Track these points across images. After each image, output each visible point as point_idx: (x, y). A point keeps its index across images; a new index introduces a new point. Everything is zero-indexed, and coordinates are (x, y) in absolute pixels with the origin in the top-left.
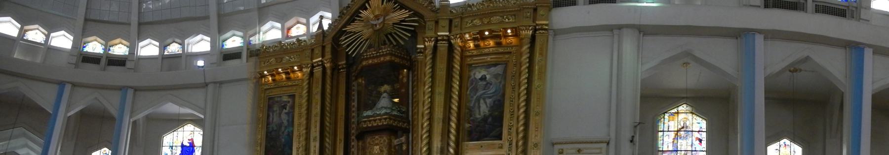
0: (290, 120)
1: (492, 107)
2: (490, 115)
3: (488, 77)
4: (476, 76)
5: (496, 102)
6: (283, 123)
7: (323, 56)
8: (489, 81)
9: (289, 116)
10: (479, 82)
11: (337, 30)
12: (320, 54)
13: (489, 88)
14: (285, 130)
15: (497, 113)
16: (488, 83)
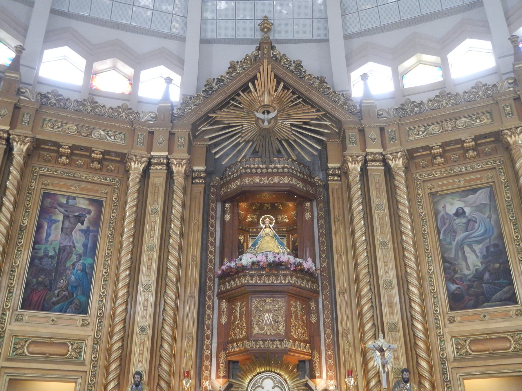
0: (89, 245)
1: (484, 257)
2: (486, 269)
3: (467, 210)
4: (447, 212)
5: (492, 249)
6: (74, 247)
7: (170, 150)
8: (469, 217)
9: (87, 238)
10: (455, 220)
11: (201, 114)
12: (166, 143)
13: (473, 229)
14: (77, 261)
15: (497, 265)
16: (469, 220)
